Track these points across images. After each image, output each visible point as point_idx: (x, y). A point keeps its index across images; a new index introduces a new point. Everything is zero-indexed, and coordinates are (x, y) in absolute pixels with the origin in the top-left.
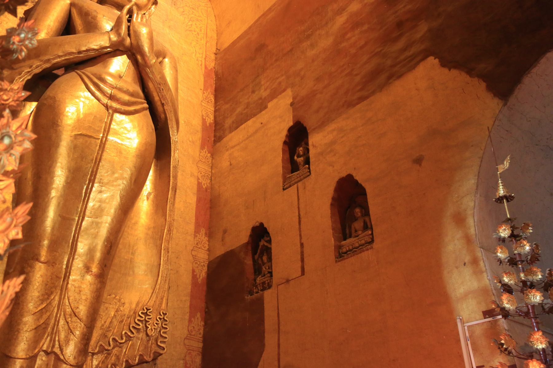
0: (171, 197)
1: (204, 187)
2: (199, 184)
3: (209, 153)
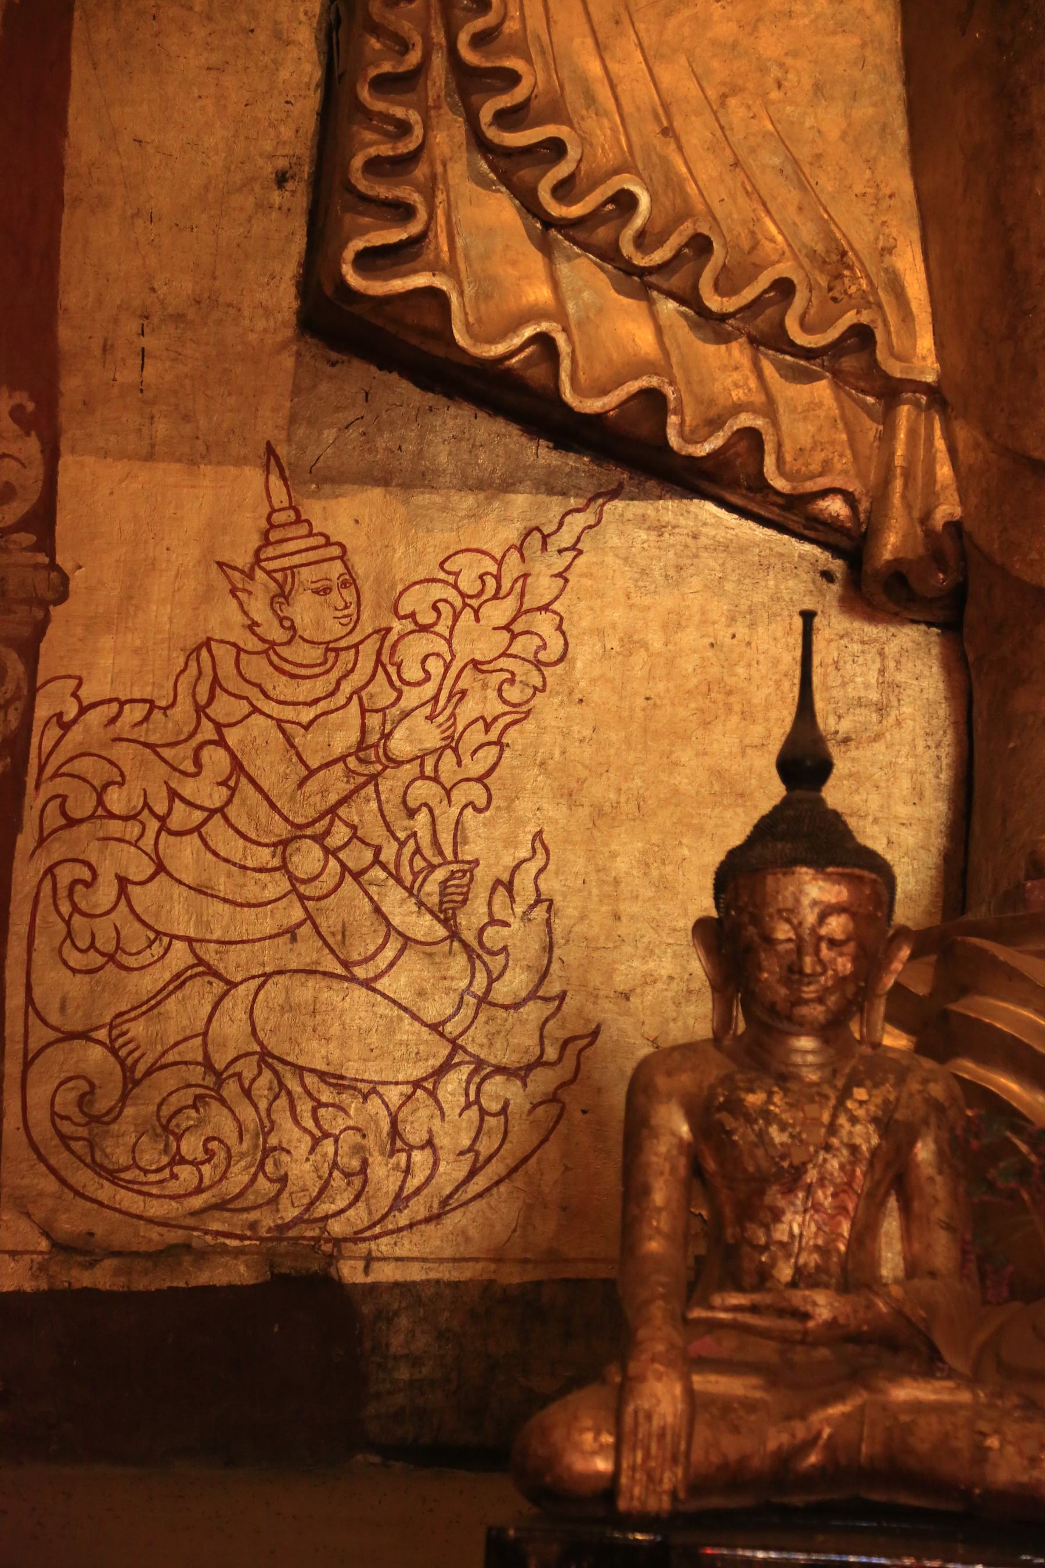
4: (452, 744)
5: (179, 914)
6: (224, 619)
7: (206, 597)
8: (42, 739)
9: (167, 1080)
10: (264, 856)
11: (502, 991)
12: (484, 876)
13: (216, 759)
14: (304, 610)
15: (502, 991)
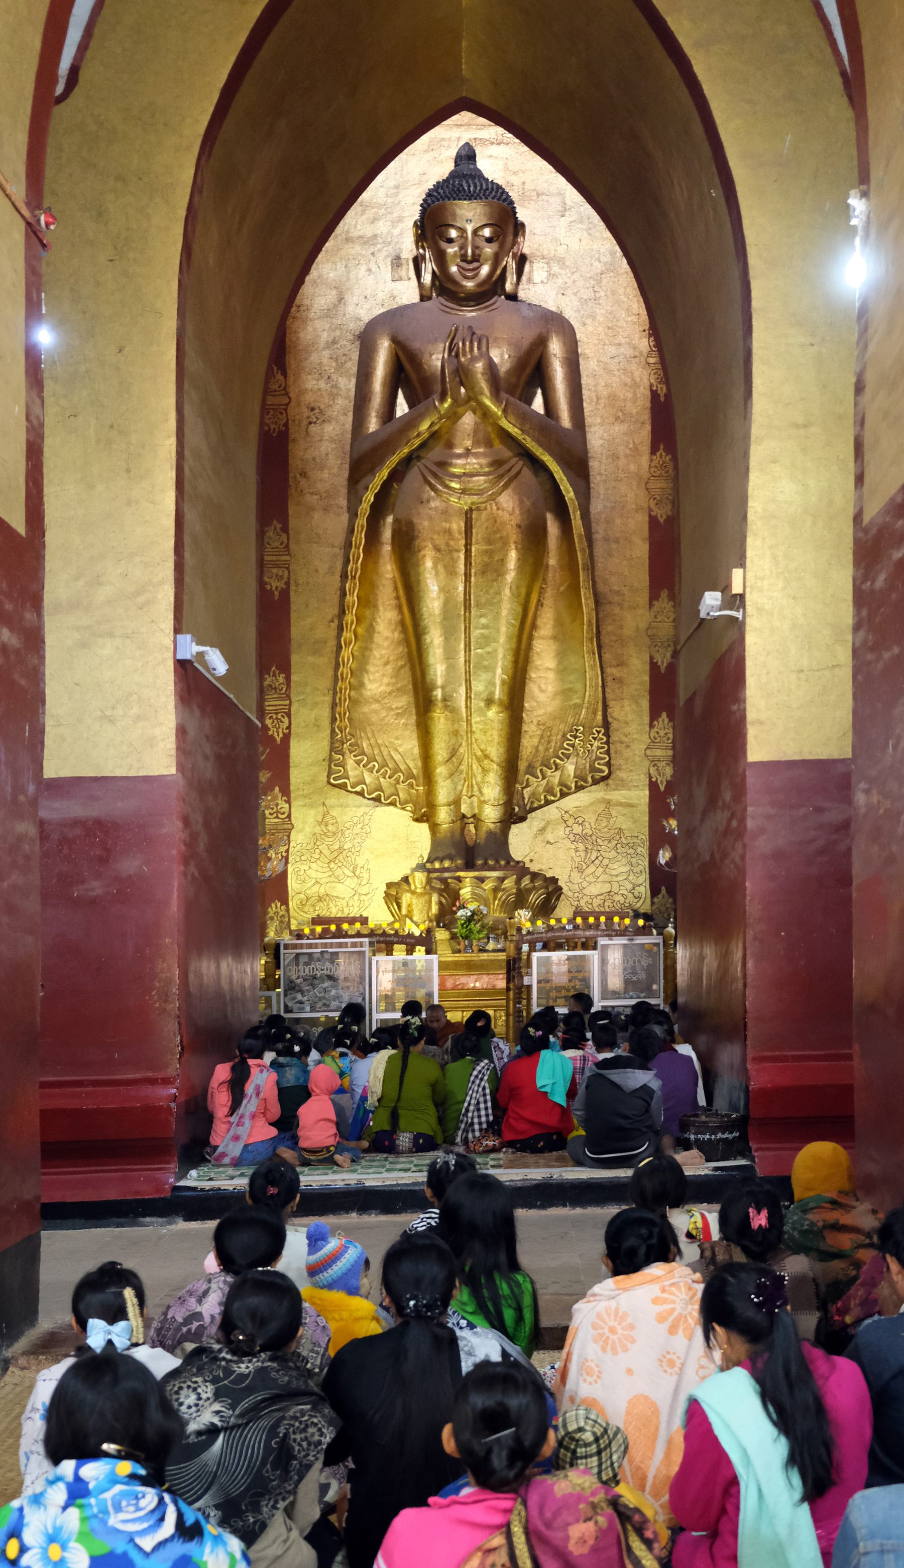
0: (584, 581)
1: (661, 520)
2: (653, 521)
3: (667, 455)
4: (354, 846)
5: (313, 875)
6: (318, 830)
7: (314, 827)
8: (291, 850)
9: (313, 899)
10: (326, 865)
11: (363, 883)
12: (359, 866)
13: (317, 851)
14: (330, 828)
15: (363, 883)
